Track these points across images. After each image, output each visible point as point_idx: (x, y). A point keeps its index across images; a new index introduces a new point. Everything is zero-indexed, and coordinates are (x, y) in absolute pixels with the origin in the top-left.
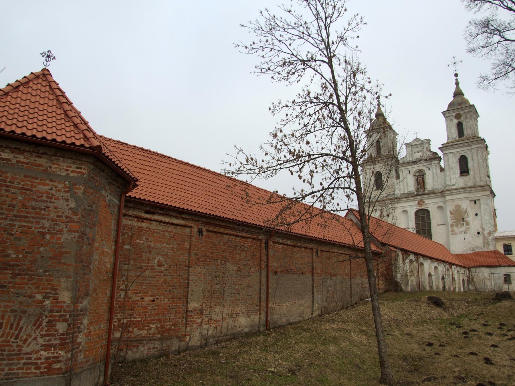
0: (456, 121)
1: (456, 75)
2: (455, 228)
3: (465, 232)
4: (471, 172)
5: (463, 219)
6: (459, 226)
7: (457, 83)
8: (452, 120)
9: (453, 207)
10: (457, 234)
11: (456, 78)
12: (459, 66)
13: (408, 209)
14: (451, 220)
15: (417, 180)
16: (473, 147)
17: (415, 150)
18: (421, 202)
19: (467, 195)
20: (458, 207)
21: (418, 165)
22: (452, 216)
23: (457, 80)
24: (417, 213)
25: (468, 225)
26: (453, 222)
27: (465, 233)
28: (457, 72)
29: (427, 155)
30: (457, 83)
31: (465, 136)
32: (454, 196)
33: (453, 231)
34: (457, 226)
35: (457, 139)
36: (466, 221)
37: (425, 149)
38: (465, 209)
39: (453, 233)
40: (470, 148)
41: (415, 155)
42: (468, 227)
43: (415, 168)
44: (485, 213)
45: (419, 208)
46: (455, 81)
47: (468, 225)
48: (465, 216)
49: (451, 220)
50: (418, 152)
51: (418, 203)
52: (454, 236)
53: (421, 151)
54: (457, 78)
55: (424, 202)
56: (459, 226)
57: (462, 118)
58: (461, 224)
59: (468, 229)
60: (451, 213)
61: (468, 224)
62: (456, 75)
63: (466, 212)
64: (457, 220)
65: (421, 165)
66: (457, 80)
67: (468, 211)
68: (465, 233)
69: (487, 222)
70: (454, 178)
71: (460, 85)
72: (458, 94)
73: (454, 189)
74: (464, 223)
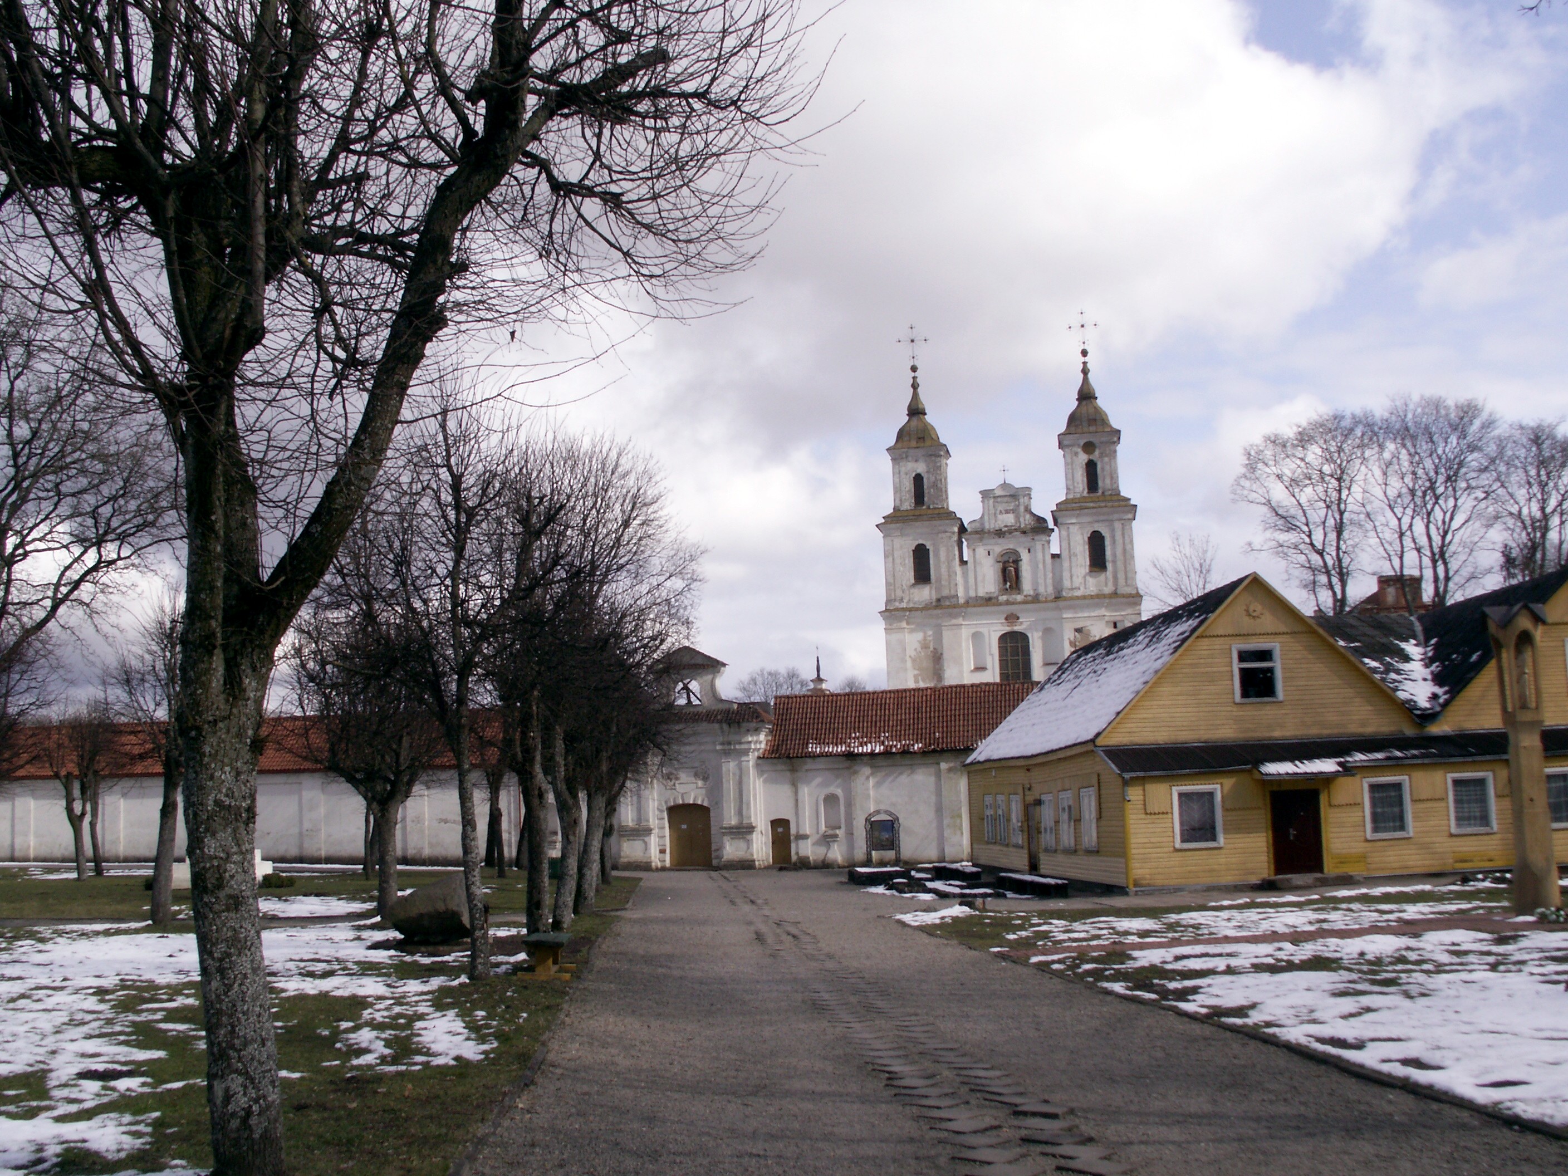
0: (1083, 458)
1: (1084, 353)
4: (1109, 566)
7: (1085, 371)
8: (1076, 454)
11: (1083, 359)
13: (984, 630)
15: (1004, 570)
17: (1001, 507)
18: (1012, 618)
19: (1103, 611)
24: (1003, 638)
28: (1086, 347)
29: (1026, 521)
30: (1085, 371)
31: (1100, 491)
35: (1085, 494)
37: (1022, 509)
41: (1000, 517)
43: (999, 547)
45: (1008, 629)
50: (1007, 512)
53: (1013, 511)
54: (1086, 359)
57: (1097, 452)
66: (1085, 363)
70: (1078, 575)
71: (1090, 375)
72: (1086, 395)
73: (1078, 598)
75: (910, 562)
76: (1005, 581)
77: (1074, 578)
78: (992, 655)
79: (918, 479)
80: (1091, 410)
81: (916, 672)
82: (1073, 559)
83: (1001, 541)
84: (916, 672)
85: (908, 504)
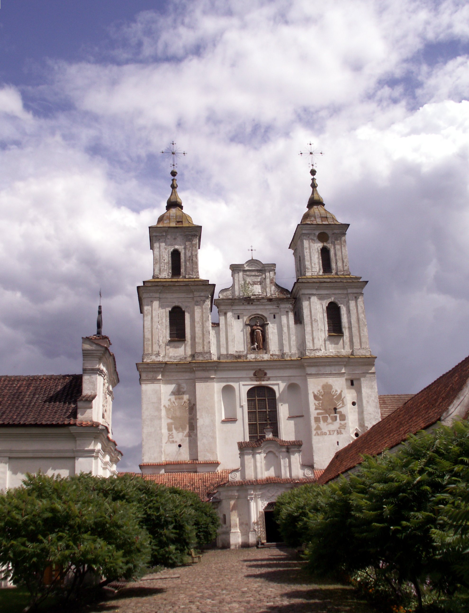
1: (313, 172)
2: (322, 424)
3: (339, 433)
4: (346, 332)
5: (335, 409)
6: (329, 420)
7: (314, 186)
9: (320, 388)
10: (325, 434)
11: (312, 177)
12: (317, 158)
13: (235, 385)
14: (316, 409)
15: (252, 333)
16: (350, 291)
20: (327, 388)
21: (255, 307)
22: (317, 402)
23: (313, 180)
24: (250, 393)
25: (344, 420)
26: (318, 414)
27: (338, 433)
28: (314, 168)
30: (314, 186)
31: (334, 272)
32: (321, 368)
33: (318, 428)
34: (325, 420)
36: (340, 412)
37: (268, 281)
38: (338, 392)
39: (319, 432)
40: (345, 292)
42: (343, 422)
44: (368, 402)
46: (311, 182)
47: (344, 420)
48: (339, 405)
49: (316, 409)
51: (255, 374)
52: (320, 438)
53: (261, 283)
54: (315, 177)
55: (265, 374)
56: (329, 420)
58: (332, 418)
59: (344, 427)
60: (316, 397)
61: (343, 418)
62: (313, 172)
63: (340, 397)
64: (326, 411)
65: (261, 307)
67: (343, 396)
68: (338, 433)
69: (372, 416)
74: (338, 415)
75: (166, 321)
76: (253, 343)
77: (316, 341)
78: (242, 407)
79: (176, 254)
80: (323, 211)
81: (170, 421)
82: (315, 325)
83: (249, 307)
84: (170, 421)
85: (166, 274)
